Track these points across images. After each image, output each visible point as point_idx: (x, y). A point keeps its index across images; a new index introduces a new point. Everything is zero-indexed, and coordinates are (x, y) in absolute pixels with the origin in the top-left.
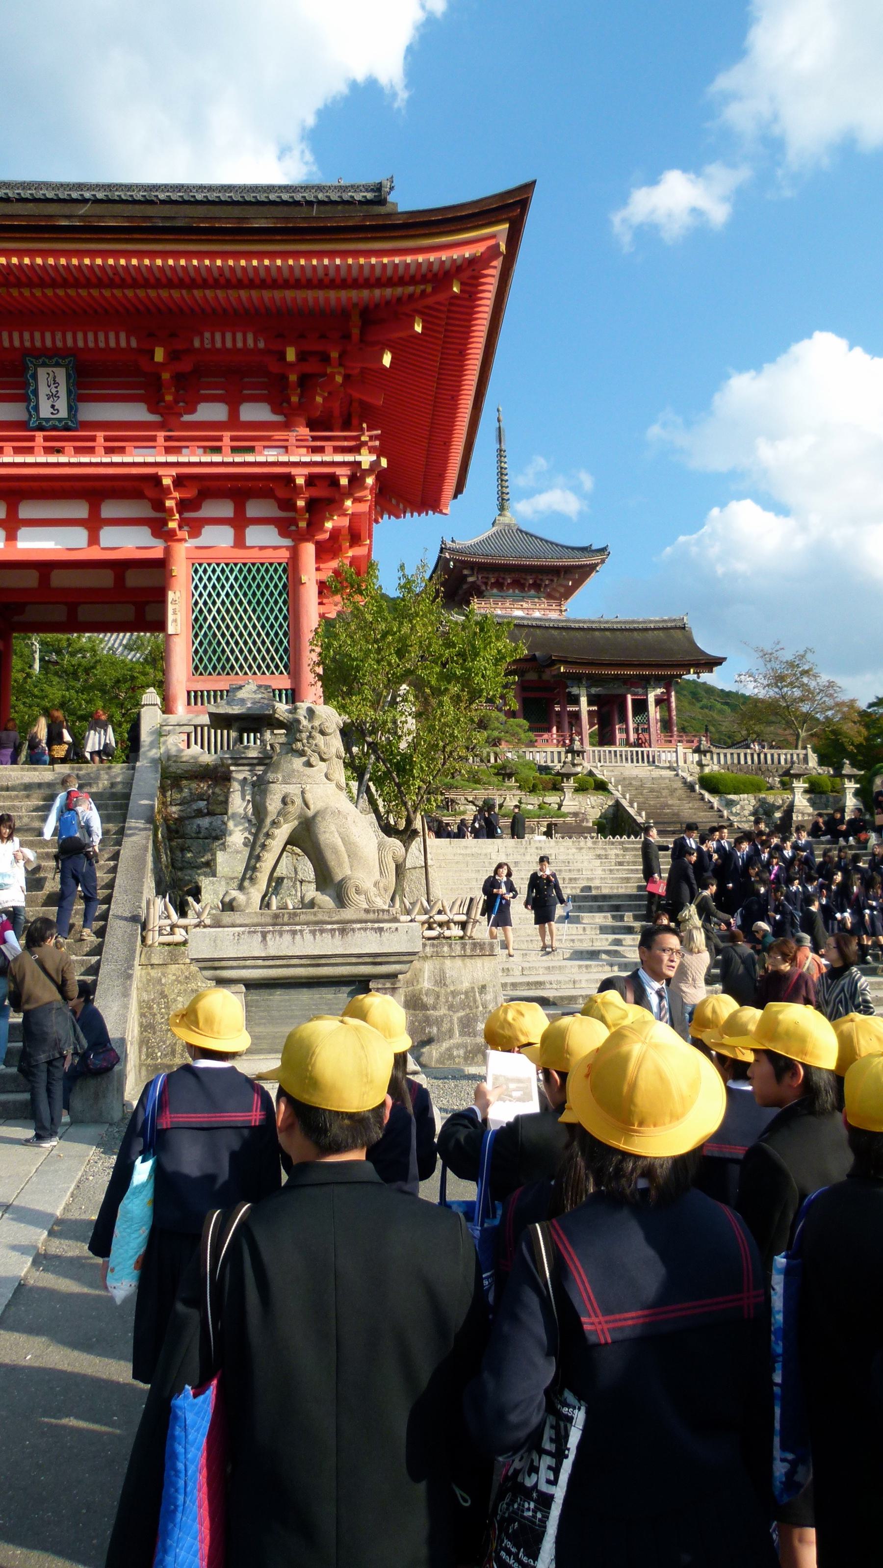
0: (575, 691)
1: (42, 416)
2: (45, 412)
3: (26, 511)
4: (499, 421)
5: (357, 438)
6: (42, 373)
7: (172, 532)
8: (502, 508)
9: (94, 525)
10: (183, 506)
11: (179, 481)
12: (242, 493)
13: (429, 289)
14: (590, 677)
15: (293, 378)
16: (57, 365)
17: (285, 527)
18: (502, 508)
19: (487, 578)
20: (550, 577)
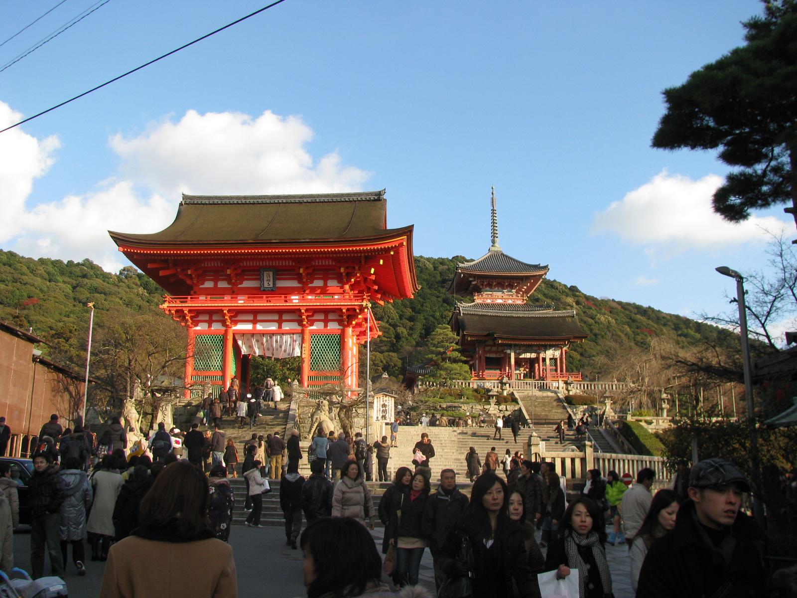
0: (508, 351)
1: (265, 286)
2: (266, 285)
3: (259, 317)
4: (492, 194)
5: (362, 296)
6: (265, 273)
7: (305, 325)
8: (493, 242)
9: (280, 322)
10: (308, 317)
11: (307, 310)
12: (327, 313)
13: (384, 253)
14: (515, 345)
15: (344, 274)
16: (270, 271)
17: (340, 322)
18: (493, 242)
19: (483, 282)
20: (518, 281)
